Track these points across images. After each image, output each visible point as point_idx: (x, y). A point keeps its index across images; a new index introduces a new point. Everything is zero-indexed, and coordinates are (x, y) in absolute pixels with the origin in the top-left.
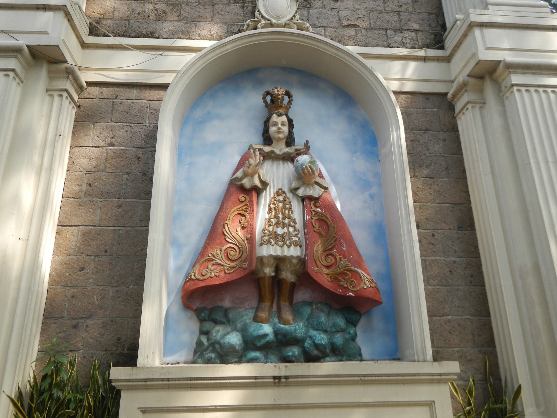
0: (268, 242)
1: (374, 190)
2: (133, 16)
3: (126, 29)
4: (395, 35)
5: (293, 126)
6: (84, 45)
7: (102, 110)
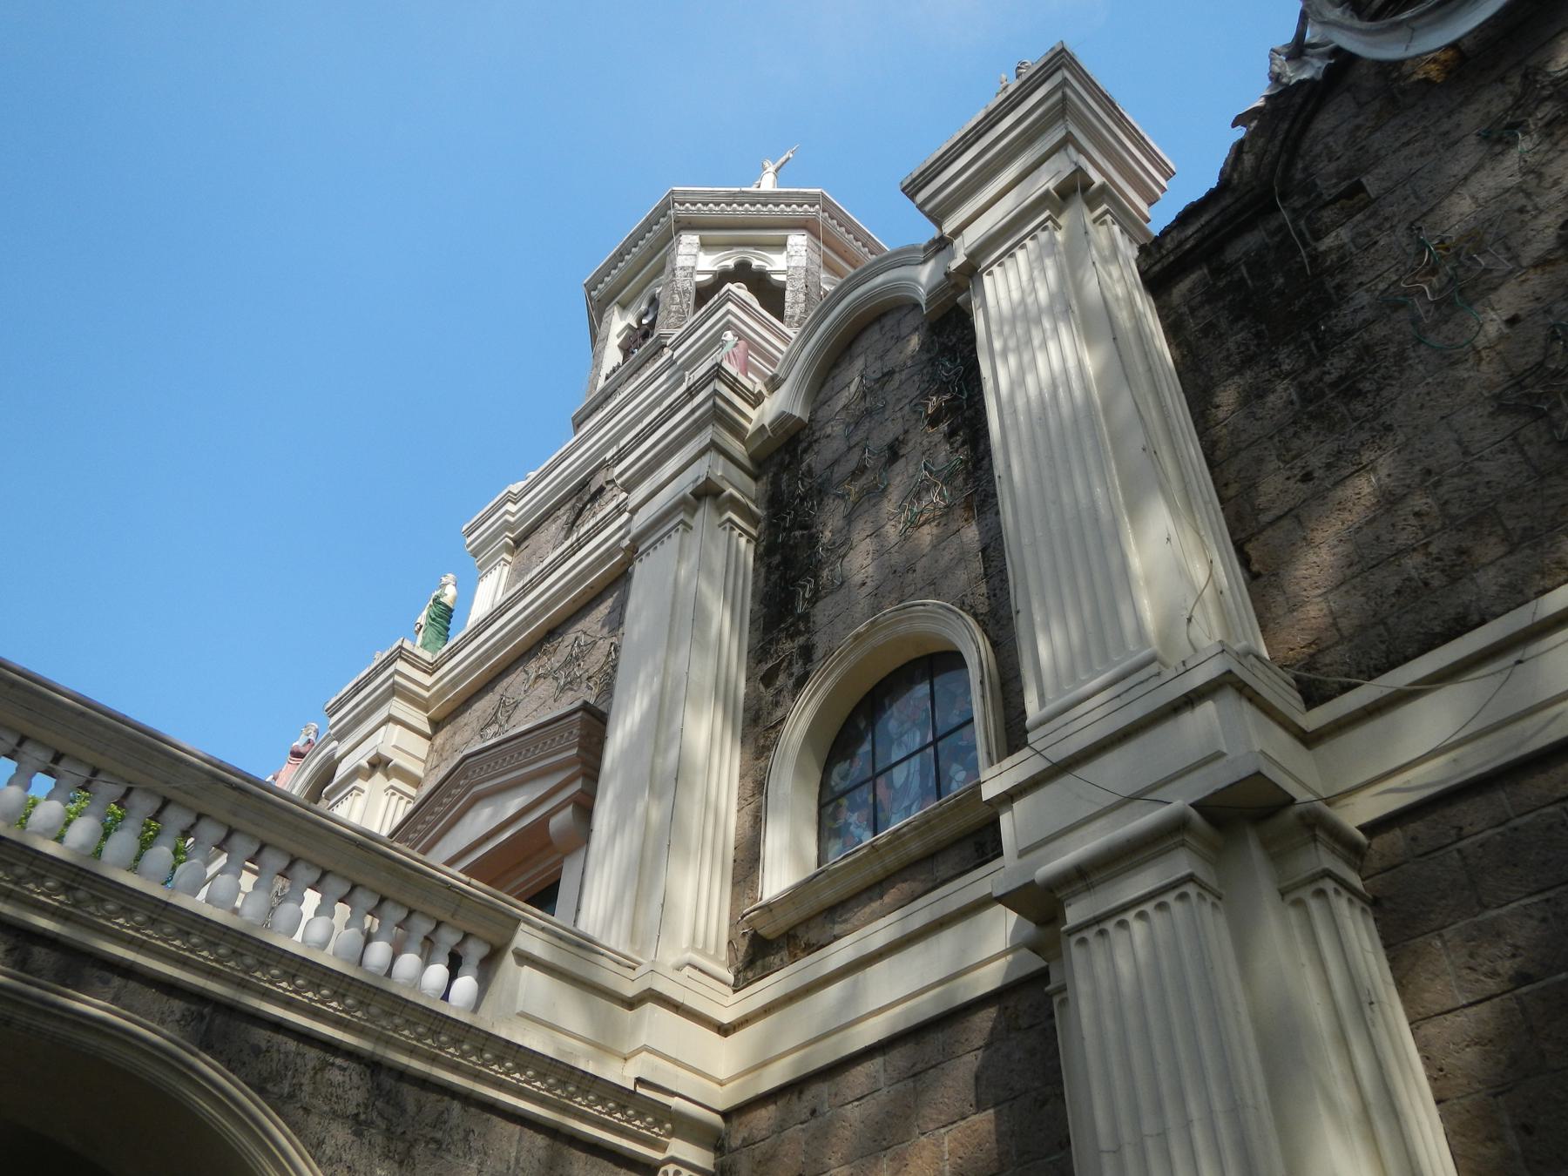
2: (1386, 606)
3: (1387, 647)
6: (1309, 740)
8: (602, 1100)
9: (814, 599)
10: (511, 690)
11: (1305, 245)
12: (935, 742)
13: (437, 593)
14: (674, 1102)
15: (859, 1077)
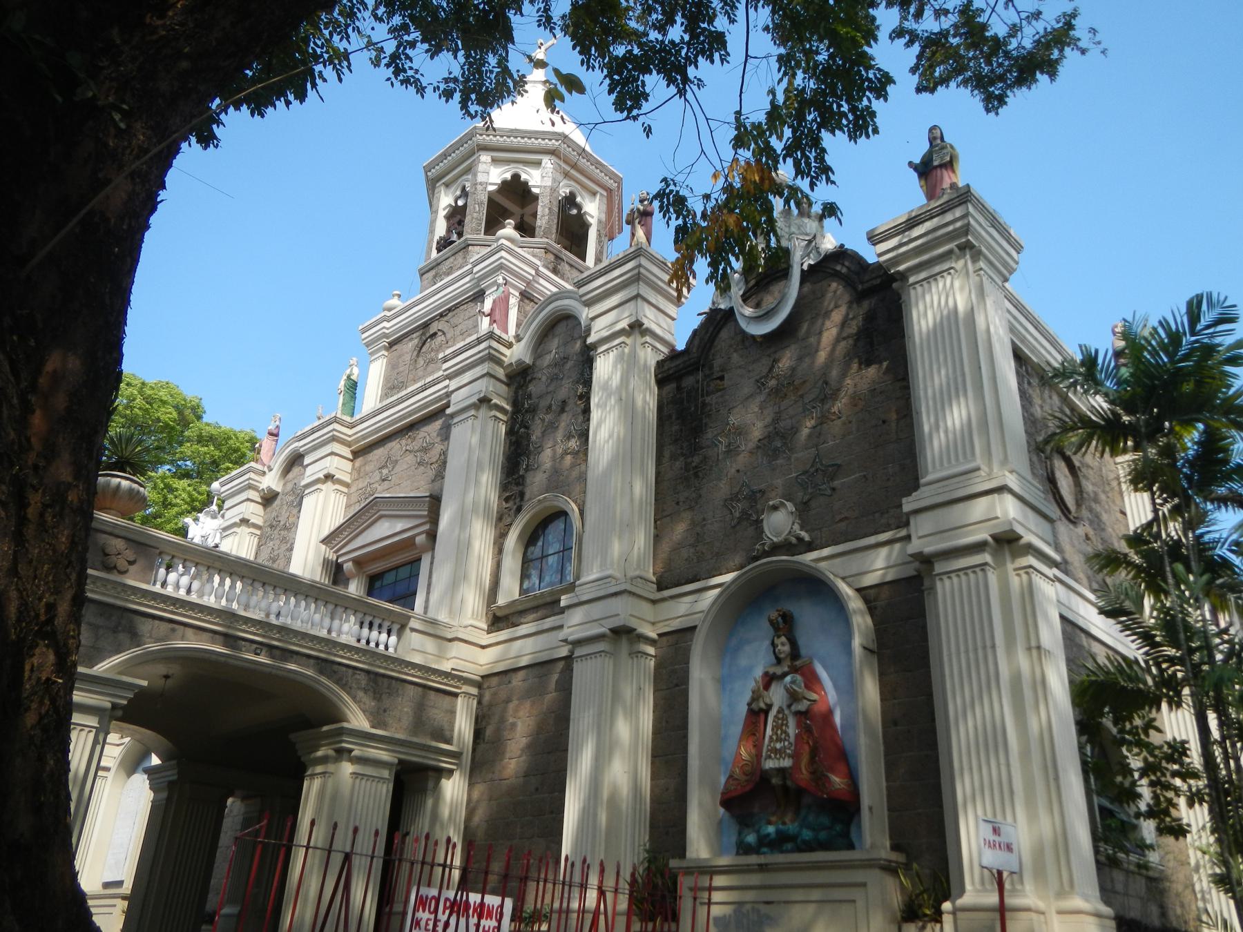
0: (770, 757)
8: (440, 676)
9: (527, 470)
10: (393, 451)
11: (703, 396)
12: (563, 551)
13: (348, 372)
14: (464, 675)
15: (521, 674)
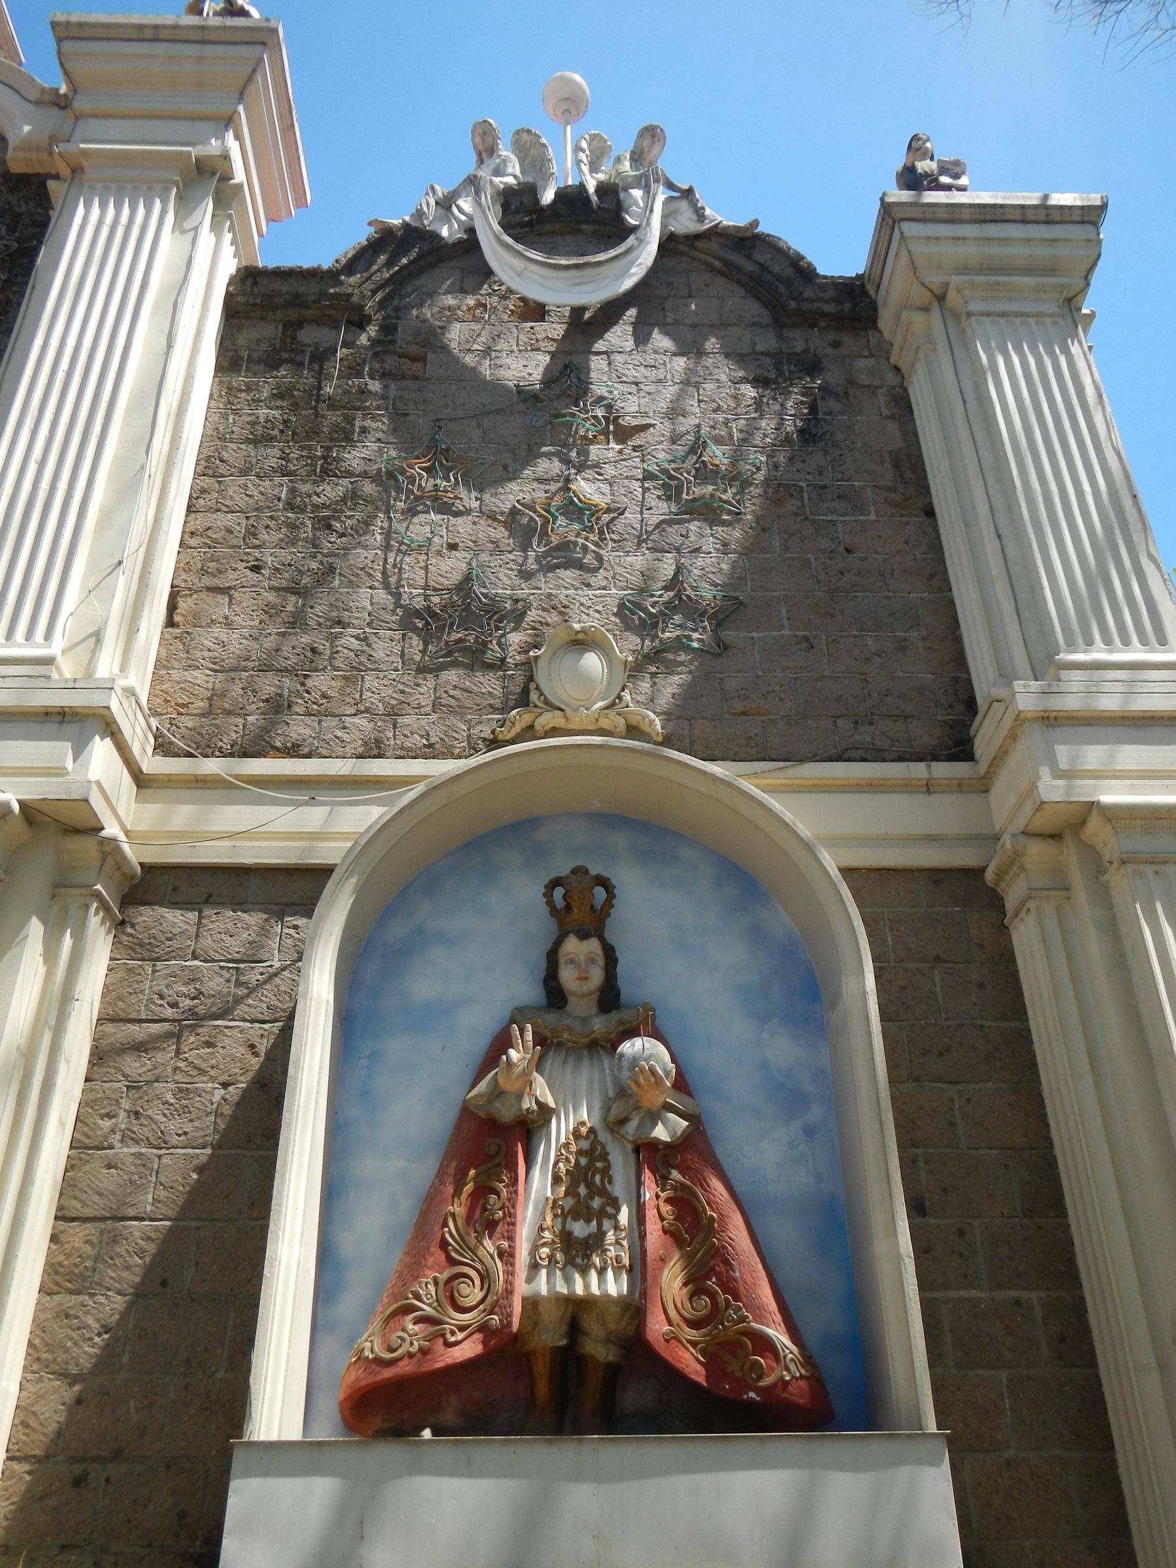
1: (815, 1114)
4: (856, 729)
5: (616, 960)
7: (173, 930)
